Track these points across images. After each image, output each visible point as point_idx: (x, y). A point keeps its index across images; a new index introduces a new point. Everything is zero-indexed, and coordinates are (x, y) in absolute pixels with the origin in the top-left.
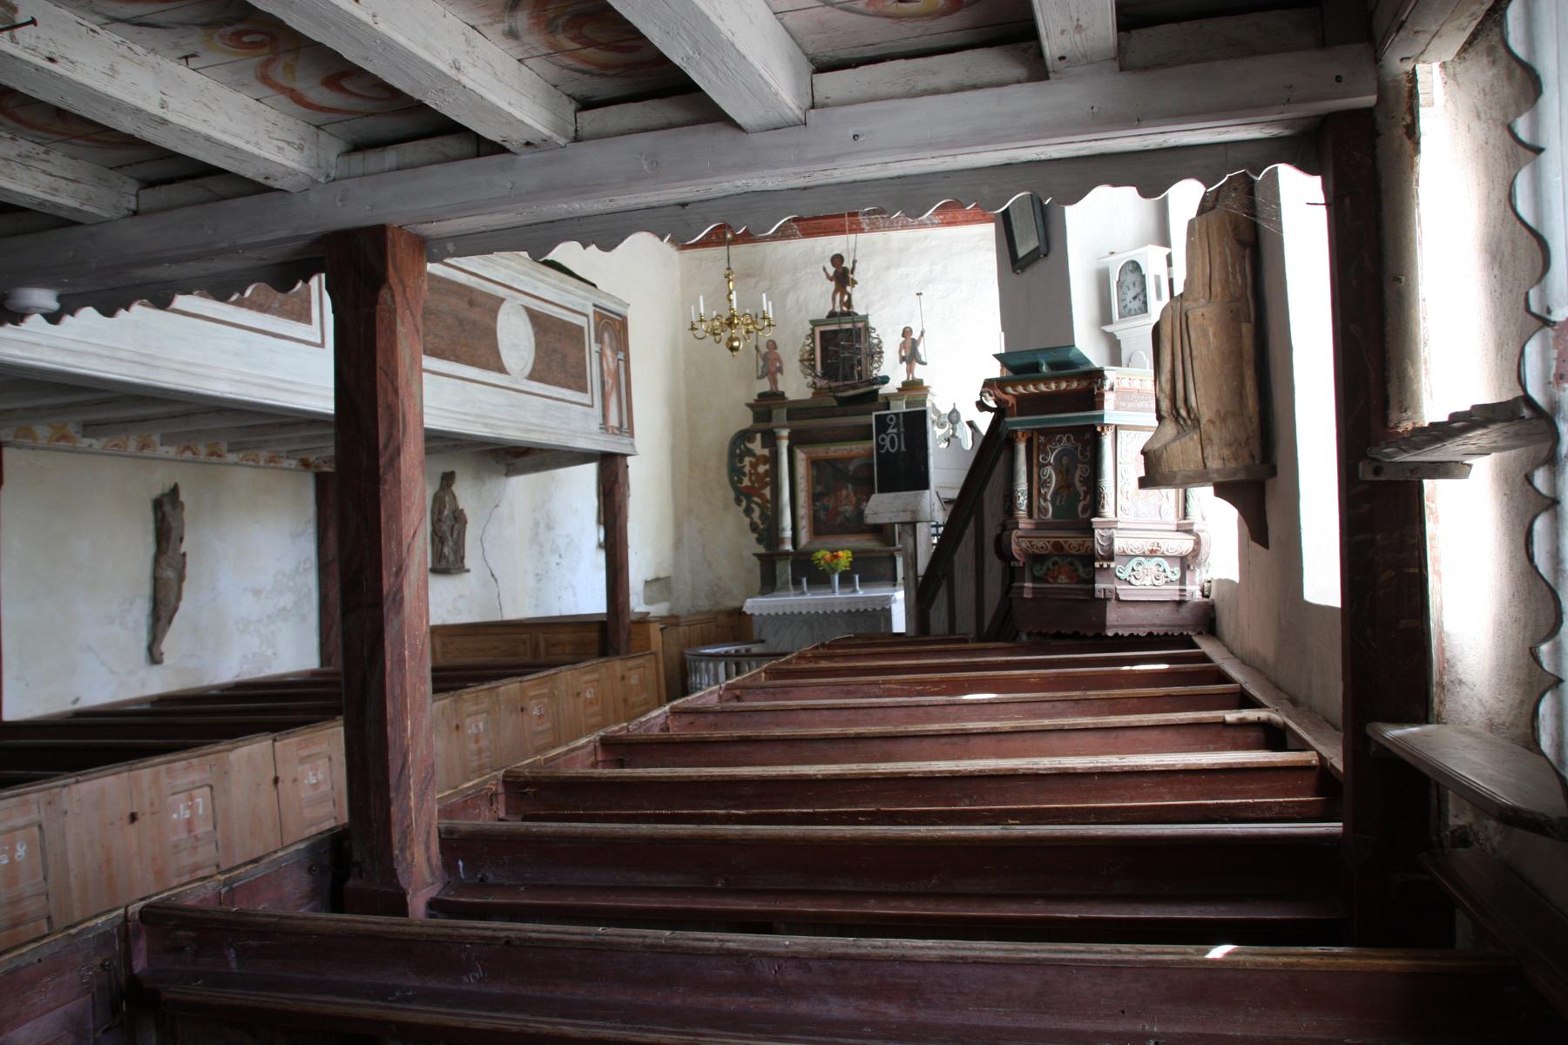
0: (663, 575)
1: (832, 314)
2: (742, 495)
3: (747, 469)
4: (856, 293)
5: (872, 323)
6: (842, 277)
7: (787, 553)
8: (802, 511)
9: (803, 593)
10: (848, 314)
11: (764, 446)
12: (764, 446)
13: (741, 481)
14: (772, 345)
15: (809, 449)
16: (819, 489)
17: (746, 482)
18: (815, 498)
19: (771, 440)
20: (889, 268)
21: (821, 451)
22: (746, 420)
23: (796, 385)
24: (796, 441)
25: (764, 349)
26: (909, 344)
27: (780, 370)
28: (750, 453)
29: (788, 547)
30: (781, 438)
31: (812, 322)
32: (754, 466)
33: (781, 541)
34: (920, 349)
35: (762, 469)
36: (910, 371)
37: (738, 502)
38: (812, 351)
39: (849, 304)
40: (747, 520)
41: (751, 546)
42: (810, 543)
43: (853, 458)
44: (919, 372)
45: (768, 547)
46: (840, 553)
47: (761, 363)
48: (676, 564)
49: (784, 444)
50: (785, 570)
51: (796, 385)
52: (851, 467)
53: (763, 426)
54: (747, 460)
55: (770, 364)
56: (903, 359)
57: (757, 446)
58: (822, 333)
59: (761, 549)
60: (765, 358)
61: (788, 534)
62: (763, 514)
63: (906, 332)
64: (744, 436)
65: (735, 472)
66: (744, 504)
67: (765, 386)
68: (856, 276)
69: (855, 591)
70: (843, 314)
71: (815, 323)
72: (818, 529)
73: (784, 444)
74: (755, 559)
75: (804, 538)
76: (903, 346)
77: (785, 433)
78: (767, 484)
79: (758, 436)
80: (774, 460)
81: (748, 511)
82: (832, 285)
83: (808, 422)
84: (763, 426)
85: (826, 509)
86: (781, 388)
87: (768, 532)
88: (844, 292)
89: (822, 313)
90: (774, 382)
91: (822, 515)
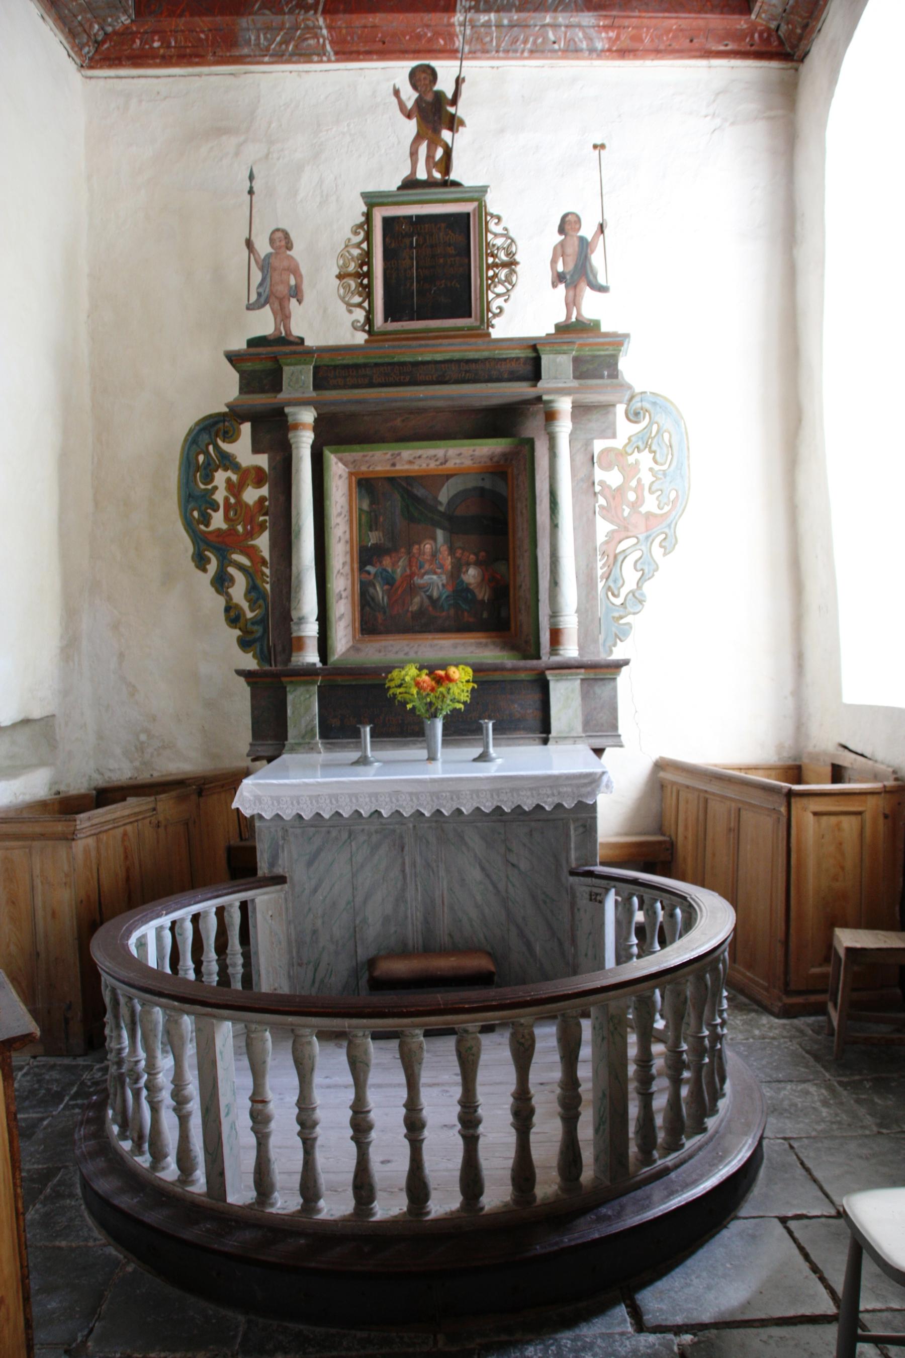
0: (36, 714)
1: (410, 184)
2: (210, 548)
3: (219, 496)
4: (461, 142)
5: (493, 204)
6: (435, 114)
7: (309, 672)
8: (341, 583)
9: (363, 761)
10: (447, 184)
11: (256, 450)
12: (256, 450)
13: (206, 519)
14: (282, 240)
15: (356, 454)
16: (374, 538)
17: (218, 521)
18: (366, 556)
19: (273, 430)
20: (502, 131)
21: (380, 460)
22: (225, 389)
23: (329, 319)
24: (333, 433)
25: (263, 247)
26: (572, 249)
27: (297, 293)
28: (228, 462)
29: (312, 657)
30: (296, 427)
31: (365, 196)
32: (235, 489)
33: (298, 644)
34: (596, 259)
35: (251, 495)
36: (572, 302)
37: (201, 562)
38: (367, 258)
39: (446, 164)
40: (221, 601)
41: (226, 657)
42: (354, 648)
43: (448, 477)
44: (592, 306)
45: (264, 657)
46: (454, 672)
47: (257, 276)
48: (66, 692)
49: (305, 441)
50: (303, 707)
51: (329, 319)
52: (444, 496)
53: (261, 400)
54: (221, 477)
55: (276, 277)
56: (559, 278)
57: (242, 448)
58: (388, 222)
59: (250, 662)
60: (266, 266)
61: (311, 629)
62: (253, 590)
63: (567, 224)
64: (215, 428)
65: (195, 502)
66: (213, 567)
67: (264, 324)
68: (461, 110)
69: (483, 757)
70: (430, 184)
71: (372, 200)
72: (370, 623)
73: (305, 441)
74: (242, 680)
75: (342, 639)
76: (560, 251)
77: (308, 416)
78: (262, 527)
79: (246, 428)
80: (282, 478)
81: (221, 582)
82: (411, 127)
83: (358, 396)
84: (261, 400)
85: (389, 580)
86: (297, 330)
87: (266, 628)
88: (435, 141)
89: (391, 183)
90: (283, 316)
91: (379, 592)
